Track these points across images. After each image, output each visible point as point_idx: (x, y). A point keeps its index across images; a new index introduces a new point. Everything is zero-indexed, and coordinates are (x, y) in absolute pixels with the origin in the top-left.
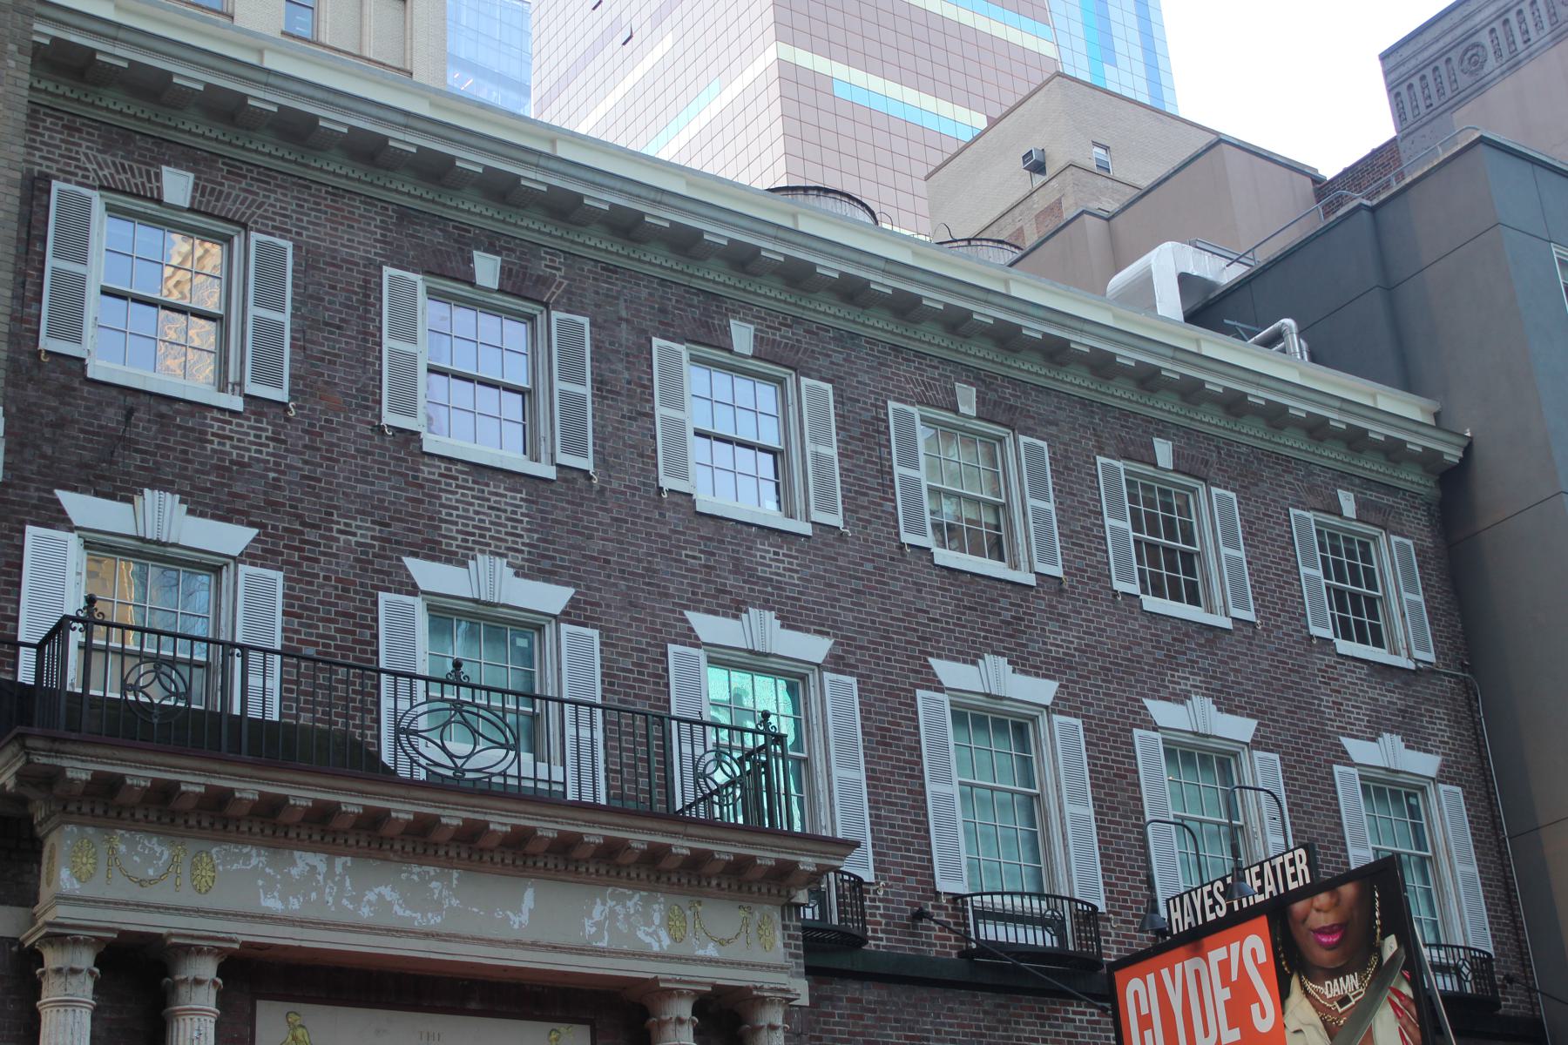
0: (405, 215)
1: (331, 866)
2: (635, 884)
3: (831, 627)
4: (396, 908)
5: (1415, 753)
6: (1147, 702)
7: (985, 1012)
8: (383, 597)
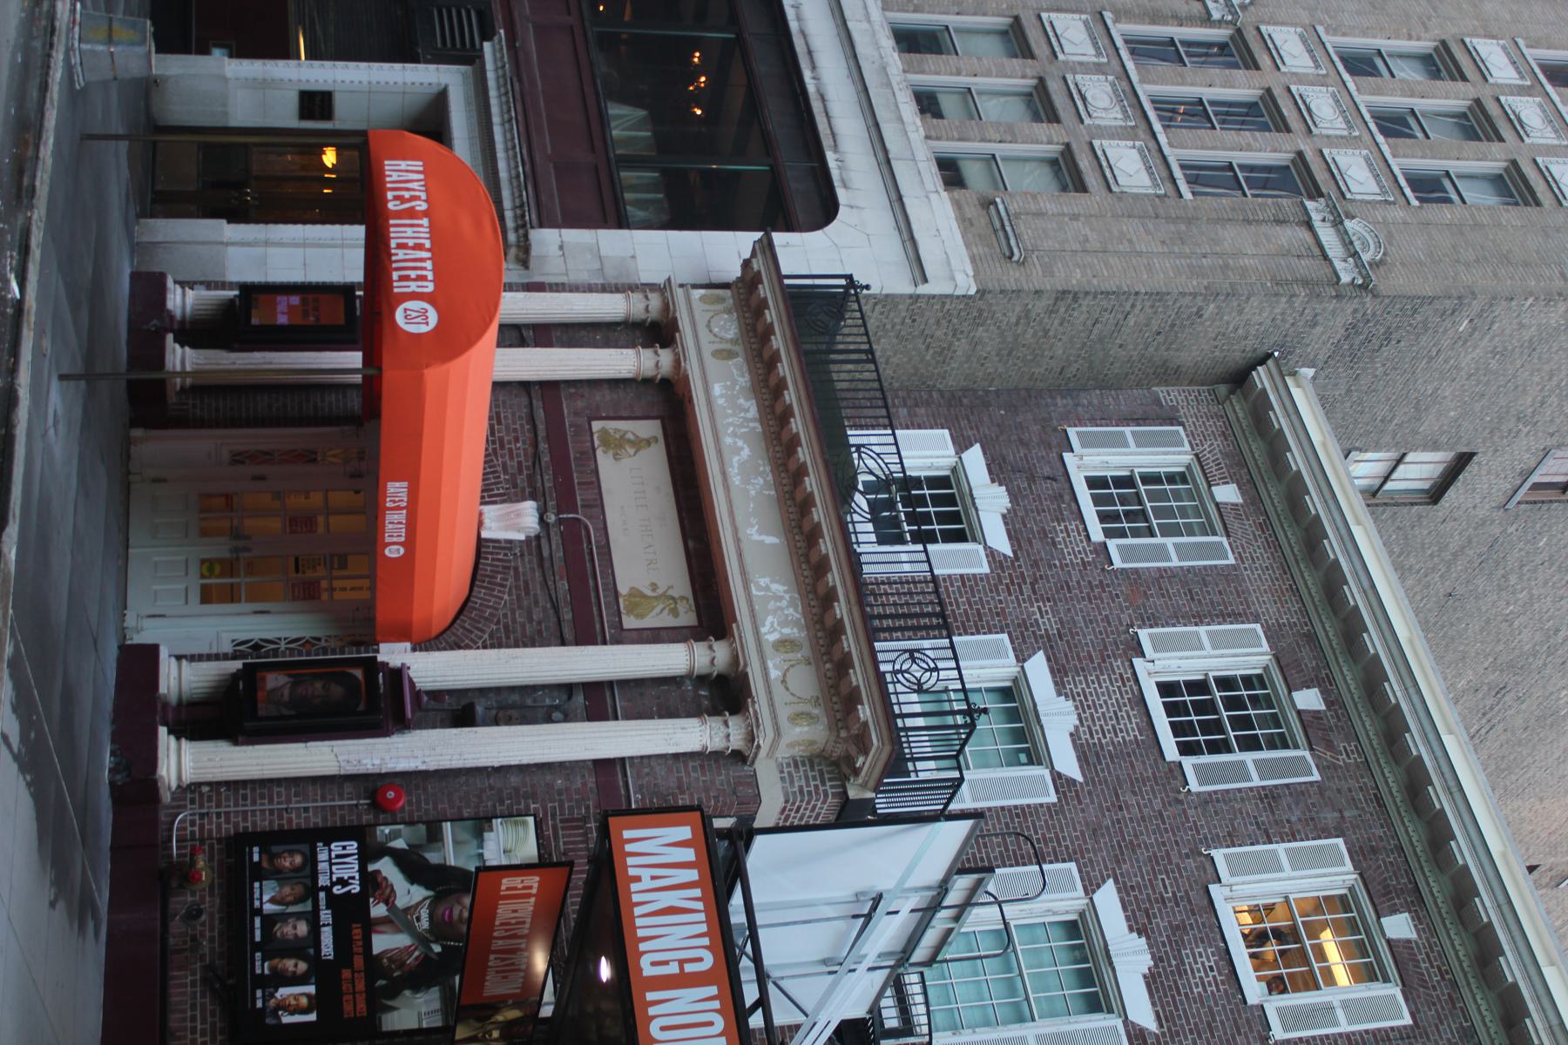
0: (1311, 638)
1: (751, 420)
2: (807, 608)
3: (1169, 1029)
4: (736, 459)
8: (1005, 636)
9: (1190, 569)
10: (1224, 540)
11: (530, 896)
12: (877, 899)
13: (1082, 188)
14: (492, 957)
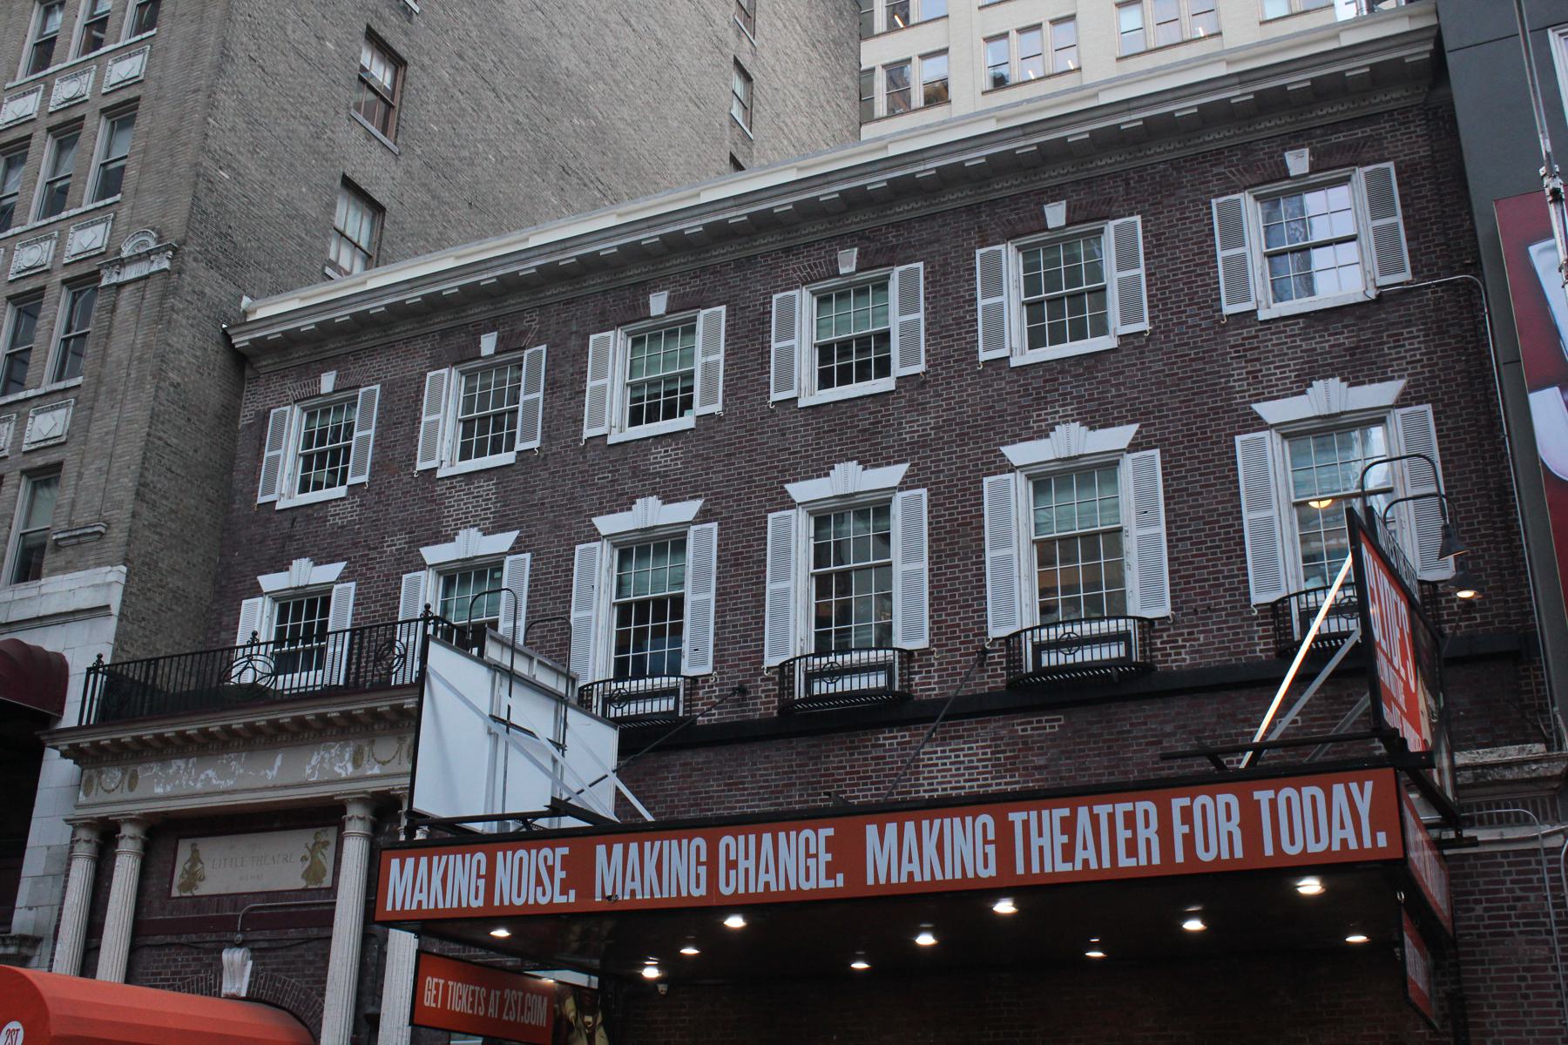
0: (445, 334)
5: (1366, 387)
6: (1005, 450)
7: (798, 754)
8: (405, 577)
9: (378, 421)
10: (362, 390)
11: (446, 987)
12: (496, 719)
13: (58, 466)
14: (505, 1017)
